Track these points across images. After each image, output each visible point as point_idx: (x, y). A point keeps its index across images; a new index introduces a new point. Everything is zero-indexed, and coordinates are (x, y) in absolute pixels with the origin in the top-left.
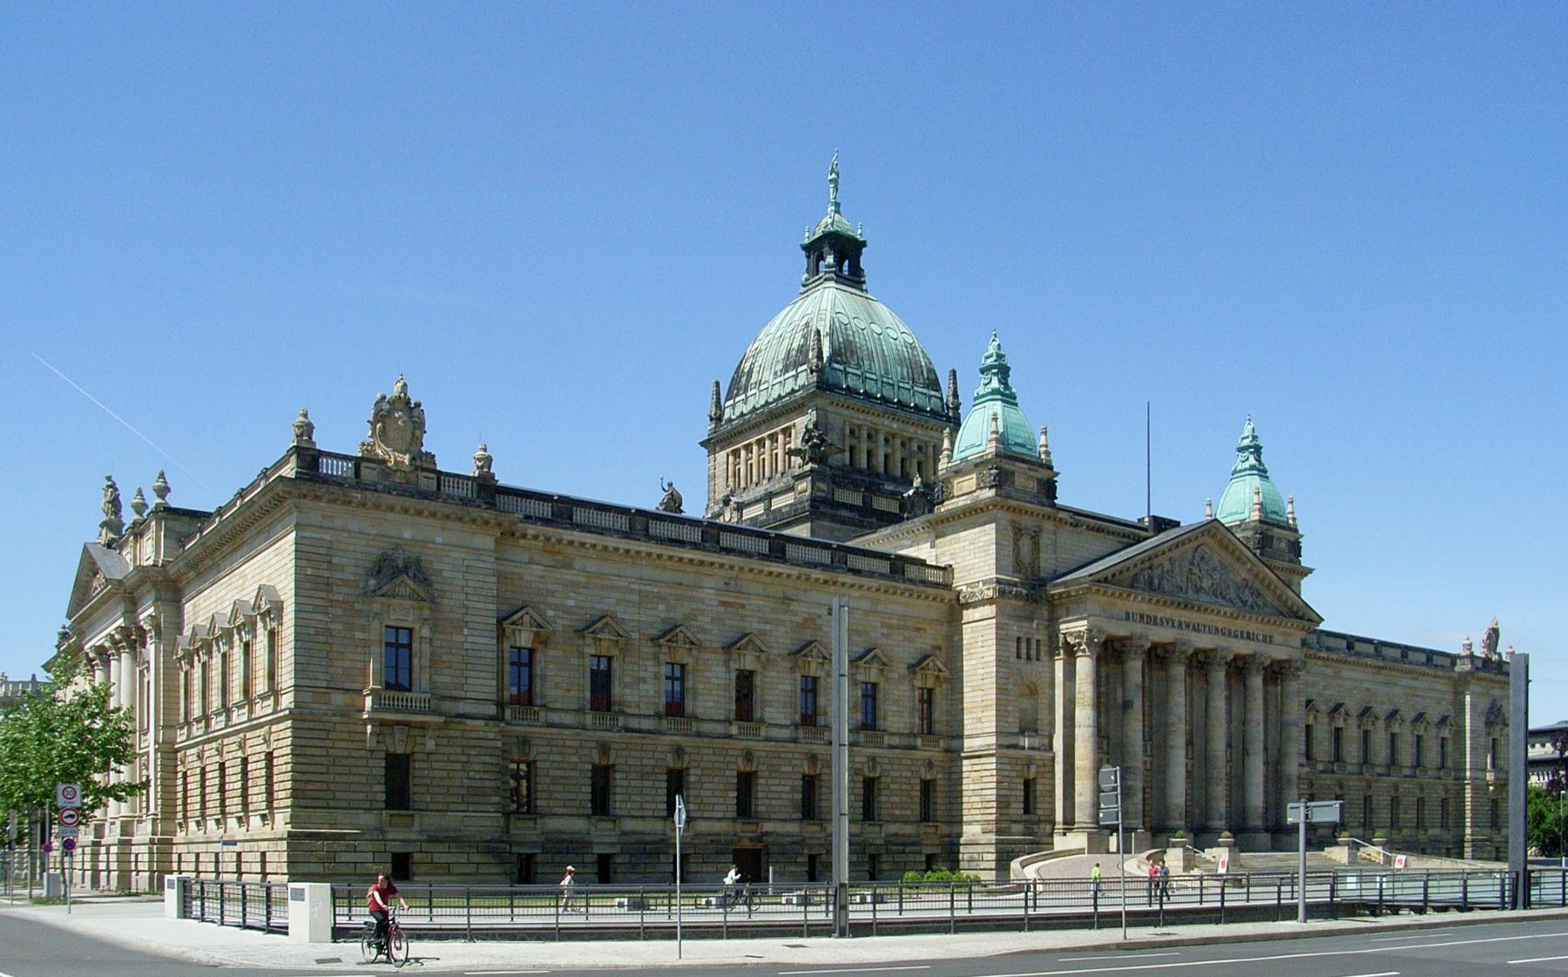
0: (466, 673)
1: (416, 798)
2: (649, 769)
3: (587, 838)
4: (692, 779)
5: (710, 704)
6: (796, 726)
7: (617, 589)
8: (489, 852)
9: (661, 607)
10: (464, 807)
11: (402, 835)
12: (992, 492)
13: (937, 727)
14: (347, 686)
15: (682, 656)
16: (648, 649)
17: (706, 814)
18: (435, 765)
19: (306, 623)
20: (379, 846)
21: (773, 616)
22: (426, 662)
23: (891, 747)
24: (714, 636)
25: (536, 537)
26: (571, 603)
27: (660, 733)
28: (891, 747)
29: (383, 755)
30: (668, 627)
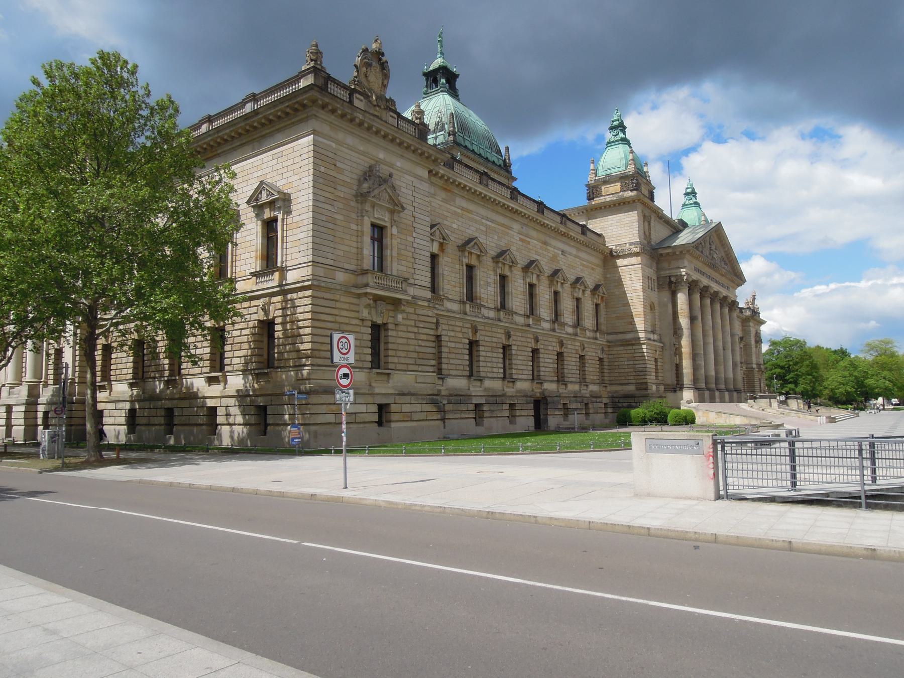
0: (416, 266)
1: (390, 359)
2: (494, 345)
3: (469, 393)
4: (514, 352)
5: (518, 304)
6: (554, 322)
7: (476, 222)
8: (434, 403)
9: (496, 237)
10: (415, 368)
11: (384, 389)
12: (634, 193)
13: (603, 328)
14: (346, 266)
15: (507, 272)
16: (490, 263)
17: (520, 377)
18: (400, 334)
19: (321, 211)
20: (370, 399)
21: (541, 251)
22: (395, 254)
23: (589, 338)
24: (522, 262)
25: (442, 177)
26: (455, 226)
27: (499, 320)
28: (589, 338)
29: (369, 324)
30: (499, 251)
